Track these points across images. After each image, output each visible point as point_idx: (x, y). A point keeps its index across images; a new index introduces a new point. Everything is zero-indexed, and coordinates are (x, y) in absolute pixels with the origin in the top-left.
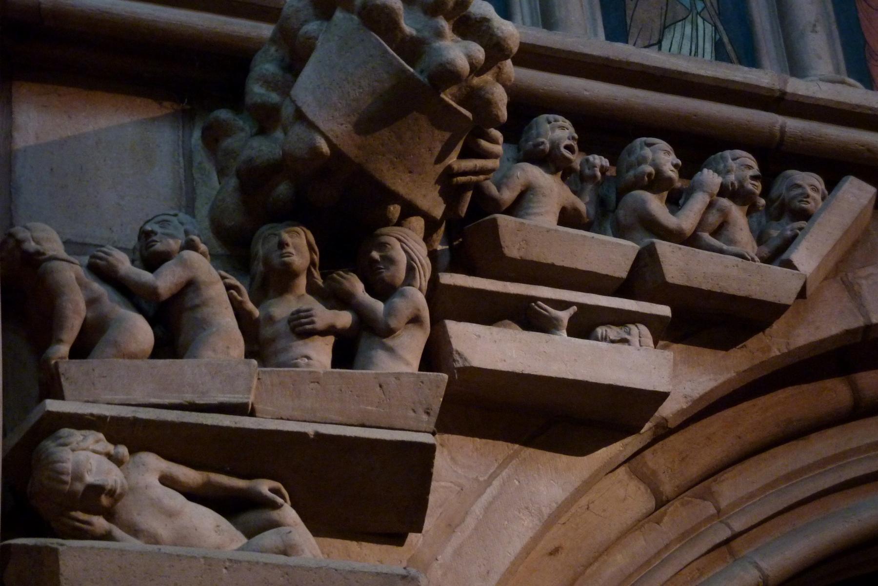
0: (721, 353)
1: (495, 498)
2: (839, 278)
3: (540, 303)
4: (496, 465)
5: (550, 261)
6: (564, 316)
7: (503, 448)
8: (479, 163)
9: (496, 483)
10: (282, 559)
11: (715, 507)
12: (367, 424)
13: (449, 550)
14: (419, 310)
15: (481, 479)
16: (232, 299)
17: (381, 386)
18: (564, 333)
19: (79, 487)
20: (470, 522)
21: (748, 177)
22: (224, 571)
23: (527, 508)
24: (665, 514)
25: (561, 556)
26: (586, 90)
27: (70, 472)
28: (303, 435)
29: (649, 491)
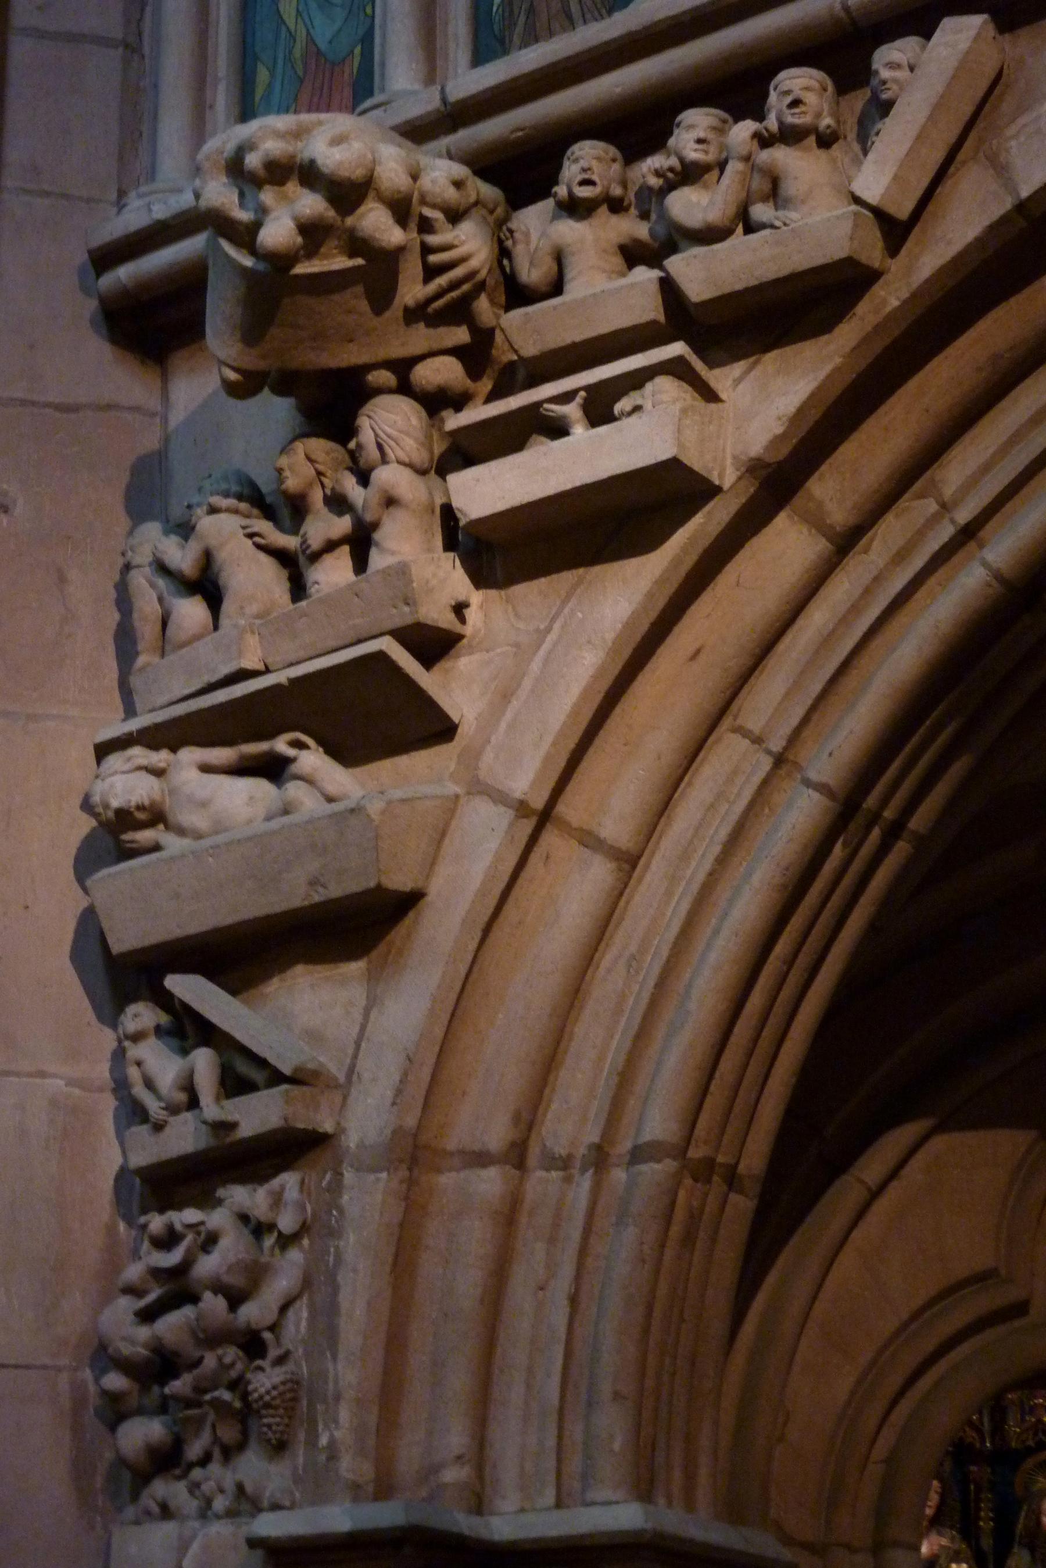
0: (825, 338)
1: (555, 644)
2: (981, 154)
3: (546, 406)
4: (558, 603)
5: (569, 341)
6: (572, 410)
7: (567, 577)
8: (442, 280)
9: (557, 626)
10: (286, 820)
11: (937, 502)
12: (361, 637)
13: (503, 725)
14: (386, 491)
15: (542, 627)
16: (259, 547)
17: (357, 595)
18: (579, 431)
19: (111, 814)
20: (527, 683)
21: (784, 108)
22: (210, 859)
23: (589, 642)
24: (876, 534)
25: (702, 658)
26: (617, 86)
27: (99, 803)
28: (278, 687)
29: (813, 531)
